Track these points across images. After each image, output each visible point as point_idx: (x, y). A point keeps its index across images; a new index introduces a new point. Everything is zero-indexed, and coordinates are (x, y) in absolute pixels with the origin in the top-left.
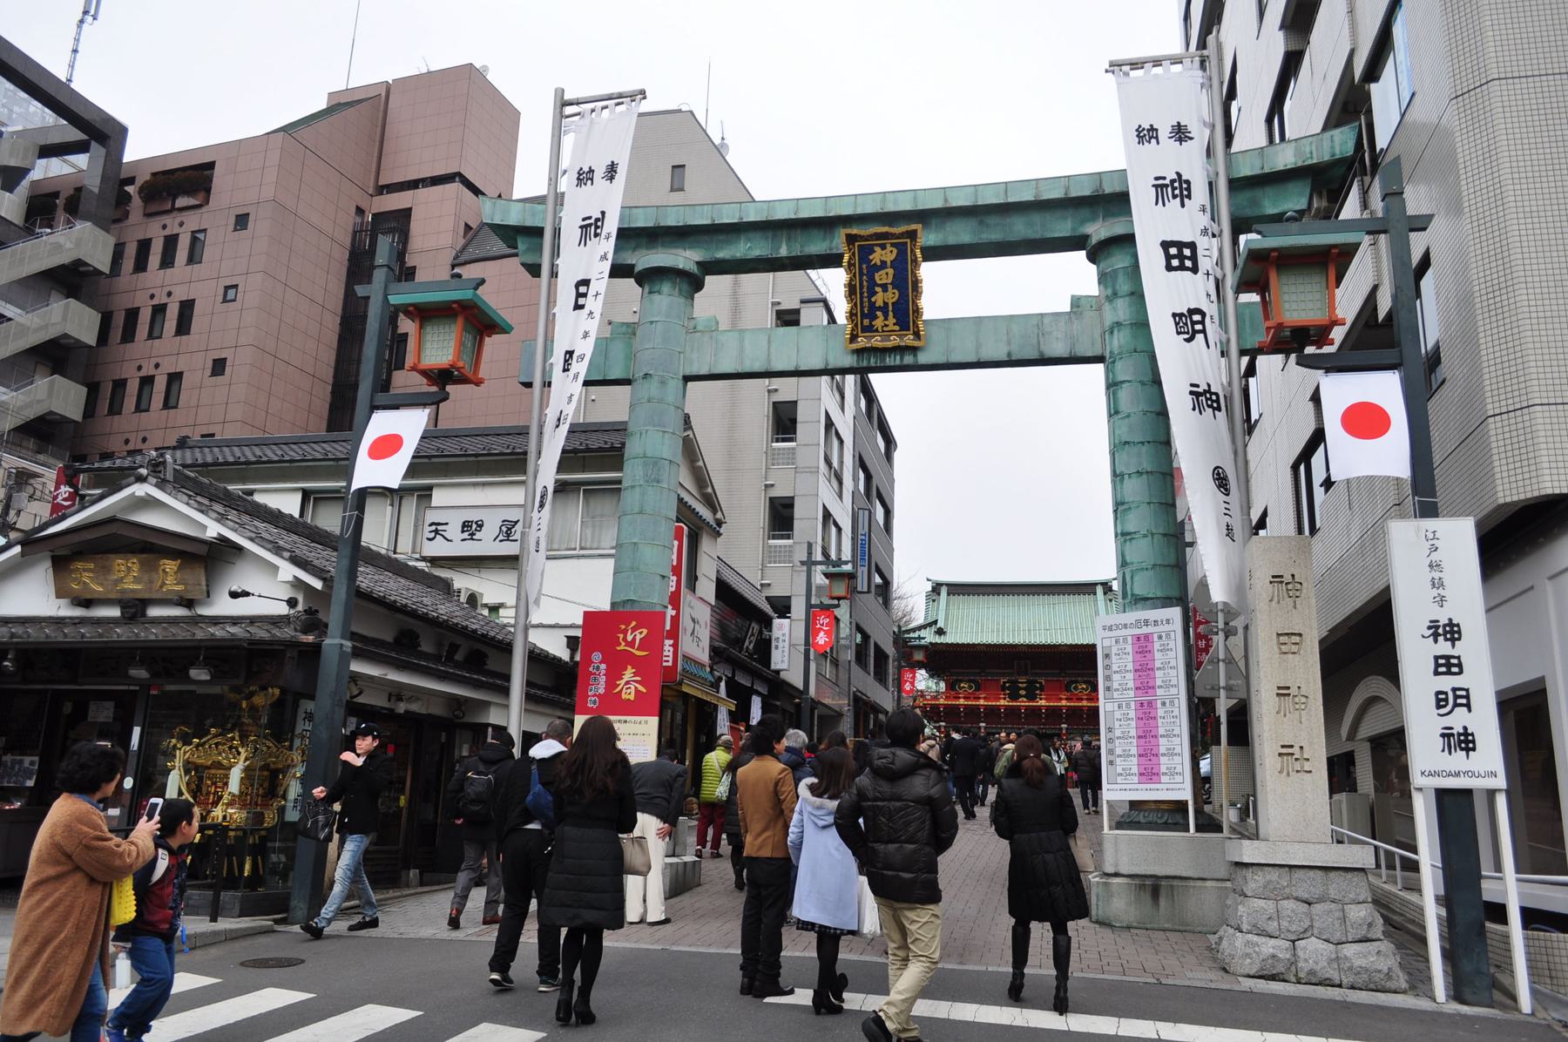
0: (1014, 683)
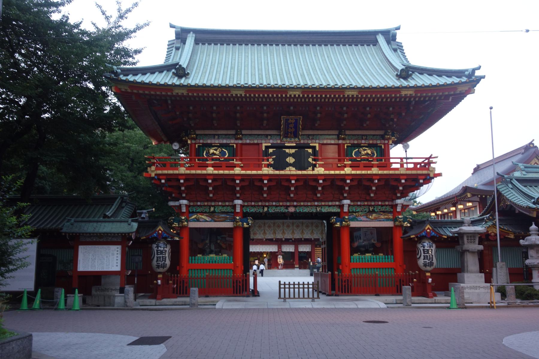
0: (280, 147)
